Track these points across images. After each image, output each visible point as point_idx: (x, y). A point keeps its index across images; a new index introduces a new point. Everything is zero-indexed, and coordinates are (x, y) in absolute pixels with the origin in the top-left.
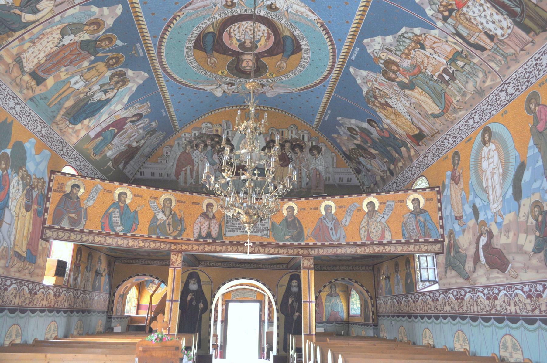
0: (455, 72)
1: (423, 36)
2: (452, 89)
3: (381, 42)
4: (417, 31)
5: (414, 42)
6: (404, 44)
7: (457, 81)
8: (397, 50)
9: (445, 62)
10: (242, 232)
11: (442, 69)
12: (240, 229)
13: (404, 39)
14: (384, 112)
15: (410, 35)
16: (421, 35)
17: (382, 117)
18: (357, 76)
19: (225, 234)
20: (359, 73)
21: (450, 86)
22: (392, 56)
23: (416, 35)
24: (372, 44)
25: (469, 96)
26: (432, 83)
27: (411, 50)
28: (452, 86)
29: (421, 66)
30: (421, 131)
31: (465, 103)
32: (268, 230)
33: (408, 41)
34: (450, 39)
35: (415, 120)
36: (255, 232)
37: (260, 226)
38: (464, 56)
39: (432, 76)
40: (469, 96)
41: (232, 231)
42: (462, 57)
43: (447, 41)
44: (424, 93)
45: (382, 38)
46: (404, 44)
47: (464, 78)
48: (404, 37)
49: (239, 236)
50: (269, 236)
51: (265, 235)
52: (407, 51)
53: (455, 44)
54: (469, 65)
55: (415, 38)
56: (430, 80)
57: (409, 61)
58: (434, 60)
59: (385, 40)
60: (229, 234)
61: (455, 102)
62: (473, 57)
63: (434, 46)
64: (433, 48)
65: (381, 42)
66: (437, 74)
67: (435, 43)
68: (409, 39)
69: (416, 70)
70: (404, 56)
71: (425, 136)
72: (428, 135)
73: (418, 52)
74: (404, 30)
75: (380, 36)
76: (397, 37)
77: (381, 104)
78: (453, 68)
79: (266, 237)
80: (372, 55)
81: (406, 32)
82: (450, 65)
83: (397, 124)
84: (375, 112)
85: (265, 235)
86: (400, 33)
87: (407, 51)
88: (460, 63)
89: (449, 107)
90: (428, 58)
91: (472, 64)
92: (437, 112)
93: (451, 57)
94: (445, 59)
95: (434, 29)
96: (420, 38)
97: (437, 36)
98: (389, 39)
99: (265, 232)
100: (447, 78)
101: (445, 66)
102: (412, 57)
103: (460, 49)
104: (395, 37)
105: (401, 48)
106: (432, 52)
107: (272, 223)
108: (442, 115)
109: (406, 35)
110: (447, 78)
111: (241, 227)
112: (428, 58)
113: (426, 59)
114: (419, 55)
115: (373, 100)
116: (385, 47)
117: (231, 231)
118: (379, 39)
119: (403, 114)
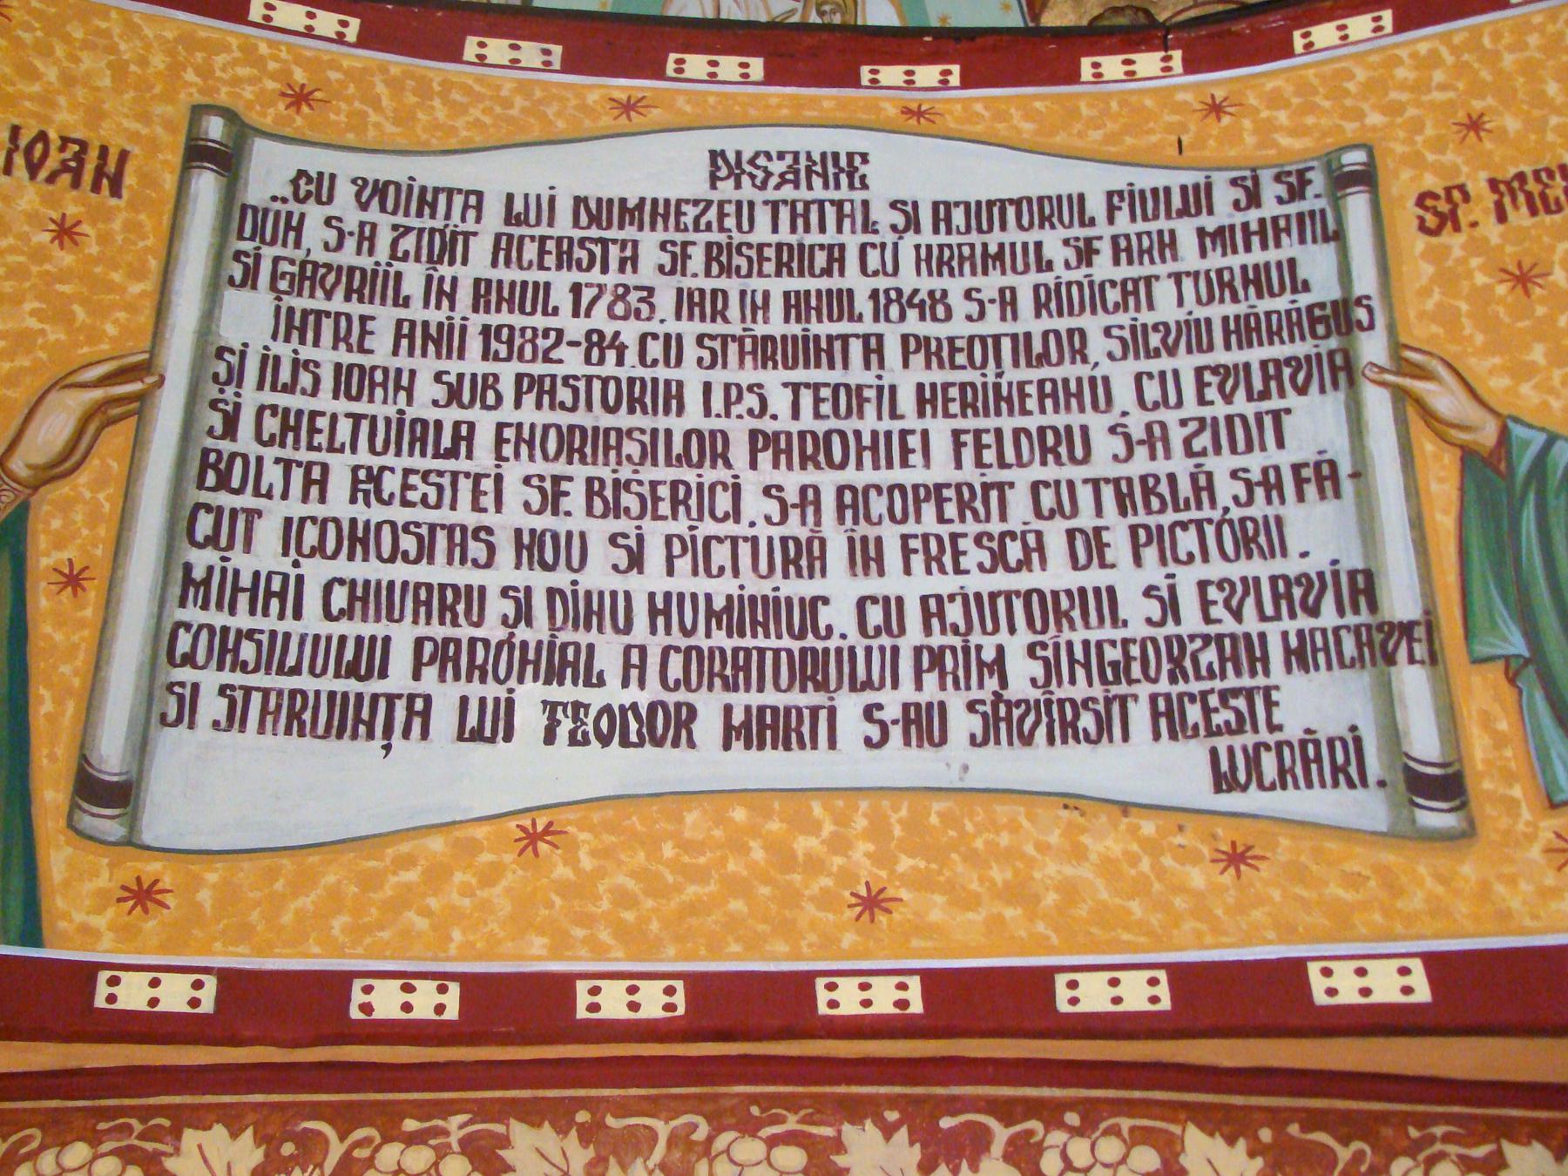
10: (615, 728)
12: (559, 664)
19: (119, 795)
32: (1382, 645)
36: (1002, 722)
37: (1129, 580)
41: (345, 721)
49: (536, 833)
50: (1447, 786)
51: (1333, 760)
60: (226, 787)
79: (1364, 808)
85: (1333, 760)
99: (1313, 703)
107: (1486, 470)
111: (588, 610)
117: (294, 716)
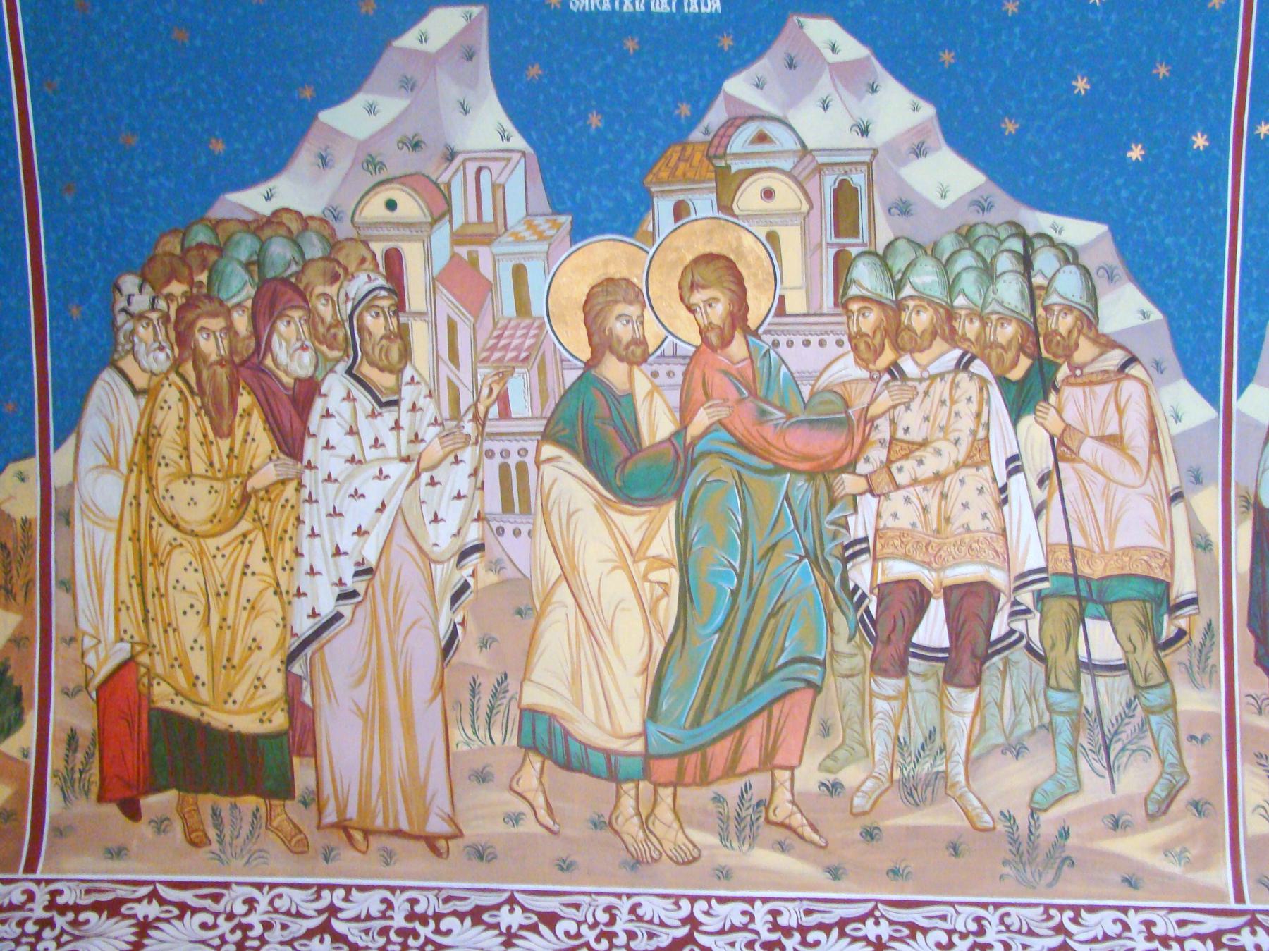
0: (1019, 654)
1: (1115, 358)
2: (892, 710)
3: (880, 135)
4: (1126, 308)
5: (1032, 333)
6: (969, 283)
7: (966, 701)
8: (883, 260)
9: (1035, 560)
11: (967, 572)
13: (1005, 263)
14: (168, 420)
15: (1069, 284)
16: (1108, 344)
17: (92, 424)
18: (408, 85)
20: (449, 90)
21: (889, 685)
22: (810, 249)
23: (1089, 320)
24: (825, 85)
25: (939, 817)
26: (803, 576)
27: (953, 338)
28: (903, 696)
29: (877, 455)
30: (301, 732)
31: (870, 834)
33: (1010, 291)
34: (1207, 504)
35: (342, 652)
38: (1168, 631)
39: (854, 550)
40: (939, 817)
42: (1149, 626)
43: (1177, 497)
44: (671, 576)
45: (921, 130)
46: (969, 283)
47: (1029, 717)
48: (1026, 262)
52: (921, 320)
53: (1201, 544)
54: (1139, 688)
55: (1064, 323)
56: (814, 558)
57: (847, 368)
58: (987, 502)
59: (919, 151)
61: (809, 776)
62: (1199, 672)
63: (1089, 449)
64: (1061, 448)
65: (880, 135)
66: (899, 569)
67: (1115, 441)
68: (1032, 294)
69: (824, 444)
70: (869, 321)
71: (284, 789)
72: (315, 799)
73: (968, 386)
74: (1080, 232)
75: (928, 110)
76: (993, 217)
77: (250, 366)
78: (1032, 627)
80: (716, 116)
81: (1069, 255)
82: (1040, 598)
83: (147, 559)
84: (105, 352)
86: (1039, 221)
87: (921, 320)
88: (1102, 641)
89: (730, 771)
90: (978, 454)
91: (1154, 698)
92: (588, 728)
93: (1094, 569)
94: (1049, 550)
95: (1209, 395)
96: (1085, 351)
97: (1168, 429)
98: (947, 178)
100: (933, 630)
101: (999, 578)
102: (894, 371)
103: (1184, 585)
104: (983, 206)
105: (926, 278)
106: (1039, 457)
108: (613, 775)
109: (1045, 261)
110: (933, 630)
112: (978, 454)
113: (952, 453)
114: (945, 404)
115: (239, 288)
116: (858, 179)
118: (898, 109)
119: (315, 552)
